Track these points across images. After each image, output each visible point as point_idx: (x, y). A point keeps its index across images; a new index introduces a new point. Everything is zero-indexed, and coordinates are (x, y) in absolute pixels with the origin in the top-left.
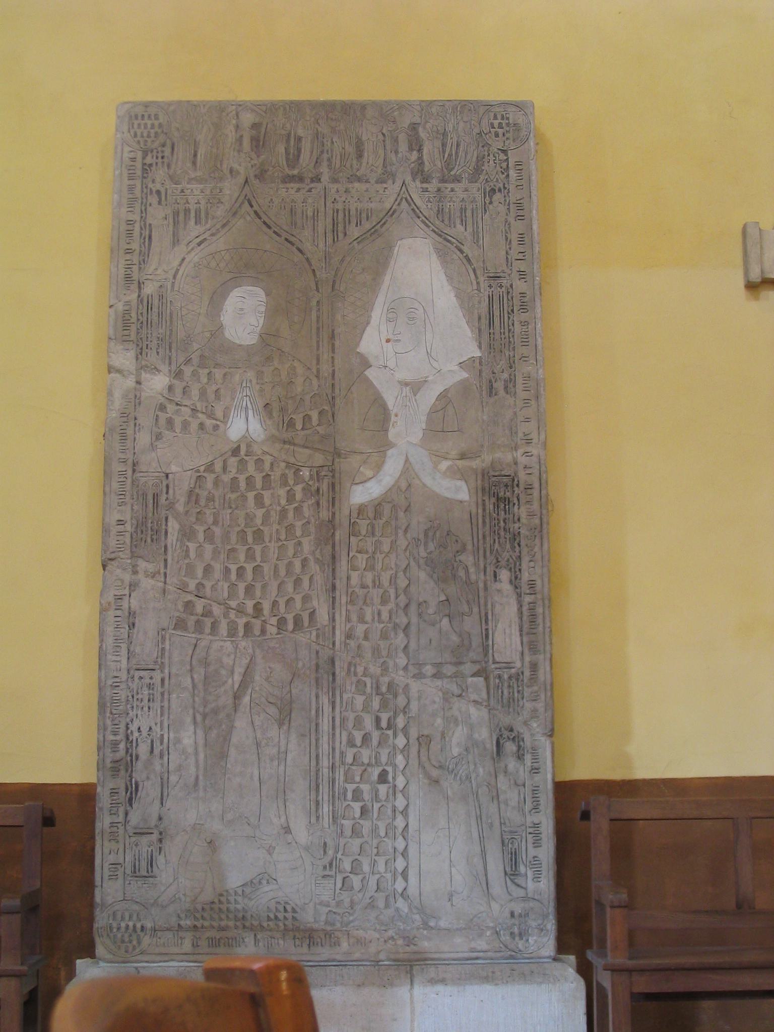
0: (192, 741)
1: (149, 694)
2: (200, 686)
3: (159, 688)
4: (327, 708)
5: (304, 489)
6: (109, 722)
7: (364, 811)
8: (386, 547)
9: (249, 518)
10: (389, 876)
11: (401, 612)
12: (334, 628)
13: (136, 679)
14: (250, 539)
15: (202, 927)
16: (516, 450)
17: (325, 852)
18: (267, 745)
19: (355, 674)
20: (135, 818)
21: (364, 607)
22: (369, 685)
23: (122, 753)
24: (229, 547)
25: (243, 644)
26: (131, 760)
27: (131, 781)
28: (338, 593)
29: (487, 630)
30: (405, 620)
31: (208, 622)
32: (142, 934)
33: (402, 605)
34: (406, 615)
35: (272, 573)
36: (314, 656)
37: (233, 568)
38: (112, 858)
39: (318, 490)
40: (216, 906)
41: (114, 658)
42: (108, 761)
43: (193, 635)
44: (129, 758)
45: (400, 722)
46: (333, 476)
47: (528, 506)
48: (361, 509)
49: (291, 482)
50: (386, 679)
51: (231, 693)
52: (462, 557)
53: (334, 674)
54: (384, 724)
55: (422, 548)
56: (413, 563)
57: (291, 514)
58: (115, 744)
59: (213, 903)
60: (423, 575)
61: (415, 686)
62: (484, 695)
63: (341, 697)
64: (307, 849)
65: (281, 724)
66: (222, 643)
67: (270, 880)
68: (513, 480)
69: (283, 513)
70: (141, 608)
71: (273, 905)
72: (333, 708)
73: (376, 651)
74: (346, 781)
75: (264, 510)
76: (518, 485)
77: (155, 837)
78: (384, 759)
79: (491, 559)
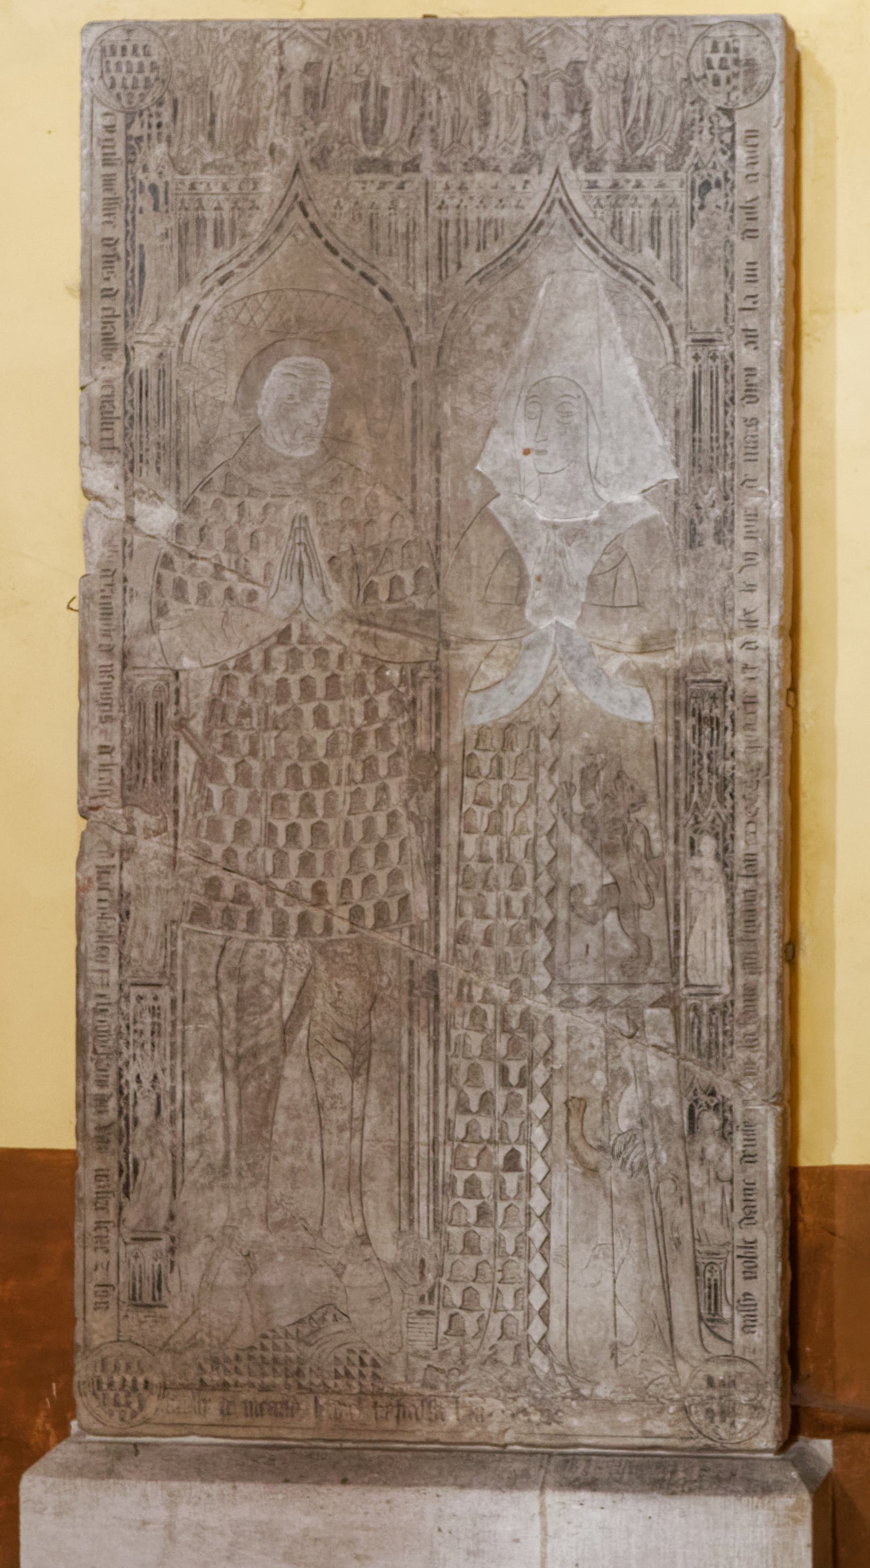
0: (218, 1097)
1: (154, 1024)
2: (231, 1013)
3: (169, 1016)
4: (426, 1053)
5: (391, 699)
6: (91, 1066)
7: (483, 1213)
8: (519, 797)
9: (307, 746)
10: (519, 1315)
11: (542, 901)
12: (437, 925)
13: (133, 999)
14: (307, 779)
15: (236, 1384)
16: (731, 639)
17: (422, 1274)
18: (333, 1107)
19: (470, 998)
20: (132, 1216)
21: (485, 893)
22: (490, 1017)
23: (112, 1114)
24: (273, 792)
25: (297, 947)
26: (127, 1126)
27: (127, 1158)
28: (443, 869)
29: (677, 932)
30: (548, 915)
31: (243, 912)
32: (146, 1394)
33: (544, 890)
34: (550, 906)
35: (341, 834)
36: (405, 968)
37: (281, 826)
38: (99, 1276)
39: (414, 701)
40: (257, 1353)
41: (98, 966)
42: (91, 1126)
43: (220, 932)
44: (123, 1123)
45: (539, 1075)
46: (438, 678)
47: (748, 733)
48: (480, 735)
49: (371, 688)
50: (518, 1008)
51: (277, 1024)
52: (641, 814)
53: (437, 998)
54: (513, 1078)
55: (576, 799)
56: (561, 823)
57: (371, 741)
58: (102, 1100)
59: (252, 1348)
60: (577, 843)
61: (562, 1019)
62: (671, 1038)
63: (448, 1034)
64: (394, 1269)
65: (354, 1073)
66: (264, 946)
67: (339, 1315)
68: (726, 688)
69: (359, 738)
70: (138, 887)
71: (342, 1353)
72: (436, 1050)
73: (502, 963)
74: (454, 1166)
75: (330, 732)
76: (732, 698)
77: (164, 1244)
78: (513, 1133)
79: (687, 817)
